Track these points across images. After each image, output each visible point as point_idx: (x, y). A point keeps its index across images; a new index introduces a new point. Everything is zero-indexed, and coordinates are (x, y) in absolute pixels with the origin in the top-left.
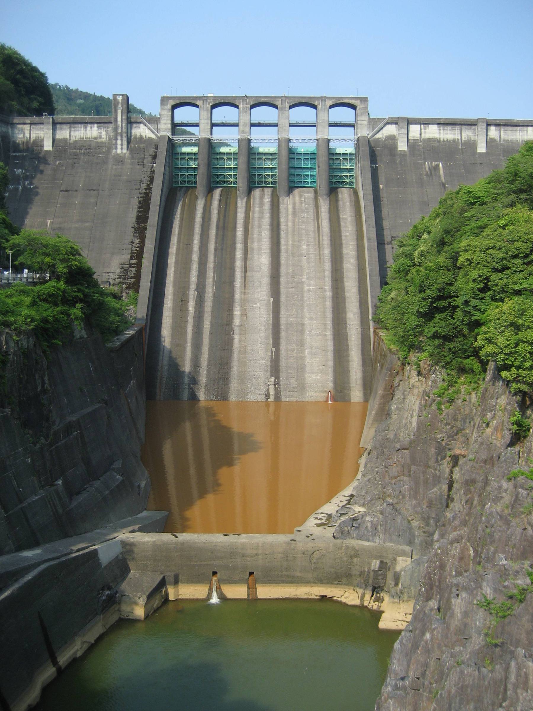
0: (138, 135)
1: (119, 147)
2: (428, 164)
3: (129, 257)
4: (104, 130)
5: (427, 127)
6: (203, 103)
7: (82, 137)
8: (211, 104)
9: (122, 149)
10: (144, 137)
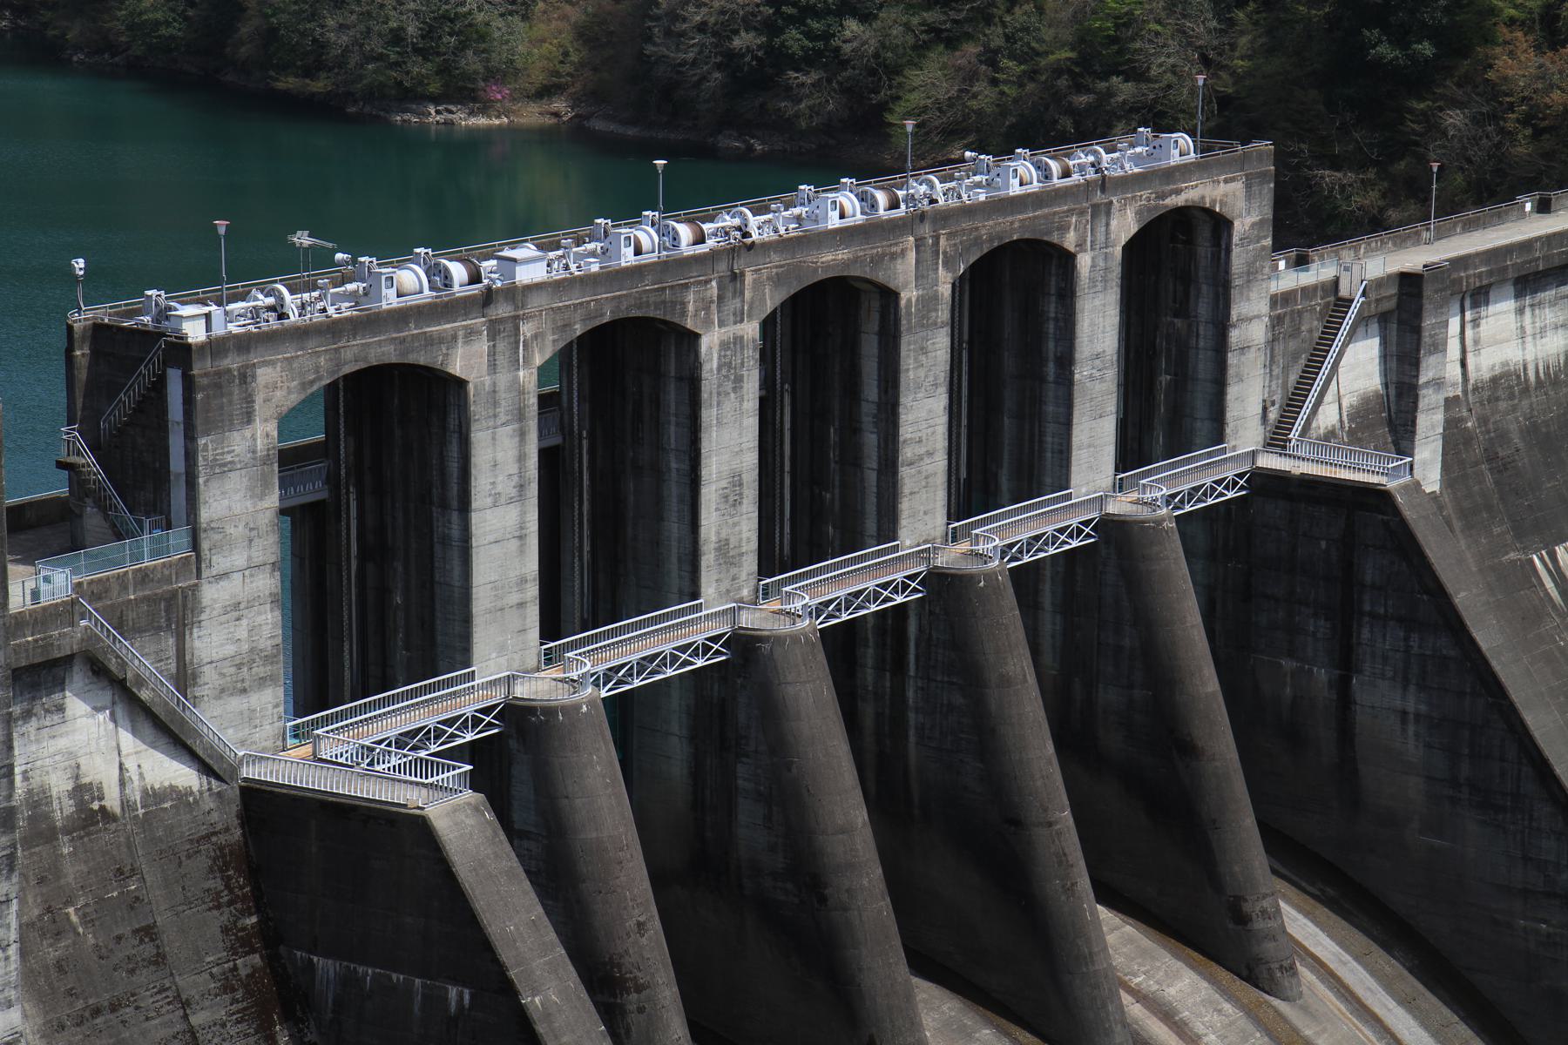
0: (59, 784)
2: (1542, 559)
5: (1483, 314)
6: (492, 353)
8: (538, 360)
10: (112, 801)
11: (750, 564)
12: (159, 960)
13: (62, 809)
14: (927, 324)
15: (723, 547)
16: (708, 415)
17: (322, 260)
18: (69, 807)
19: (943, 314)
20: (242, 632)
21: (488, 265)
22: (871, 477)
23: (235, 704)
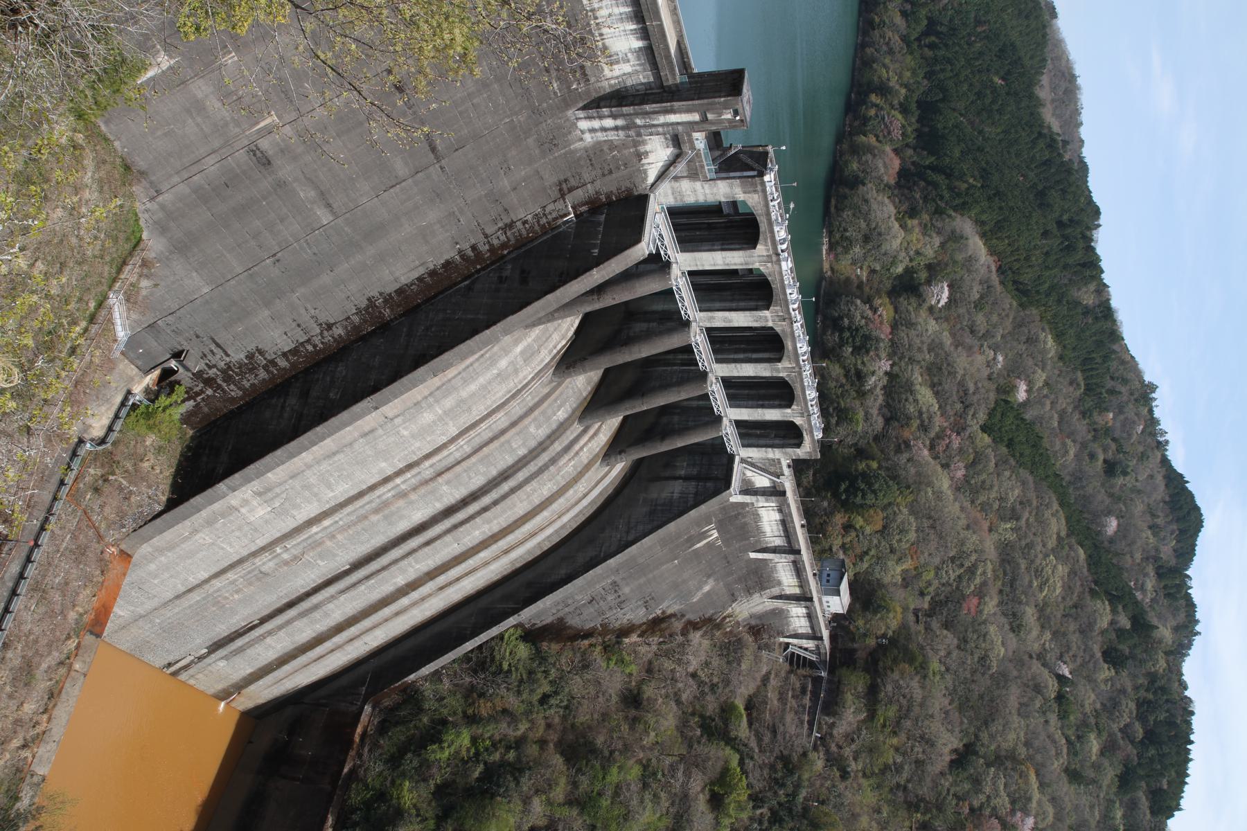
0: (648, 148)
1: (596, 124)
3: (286, 349)
4: (638, 68)
7: (599, 14)
9: (592, 130)
10: (644, 161)
11: (709, 325)
12: (604, 175)
13: (642, 149)
14: (772, 370)
15: (713, 318)
16: (748, 313)
17: (787, 211)
18: (642, 150)
19: (775, 374)
20: (688, 193)
21: (786, 254)
22: (732, 356)
23: (670, 192)
